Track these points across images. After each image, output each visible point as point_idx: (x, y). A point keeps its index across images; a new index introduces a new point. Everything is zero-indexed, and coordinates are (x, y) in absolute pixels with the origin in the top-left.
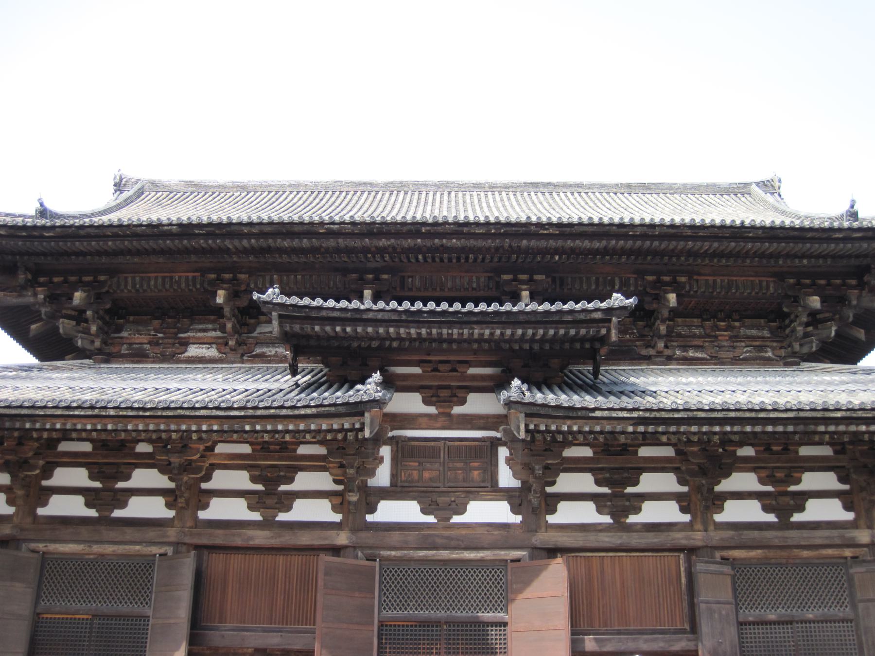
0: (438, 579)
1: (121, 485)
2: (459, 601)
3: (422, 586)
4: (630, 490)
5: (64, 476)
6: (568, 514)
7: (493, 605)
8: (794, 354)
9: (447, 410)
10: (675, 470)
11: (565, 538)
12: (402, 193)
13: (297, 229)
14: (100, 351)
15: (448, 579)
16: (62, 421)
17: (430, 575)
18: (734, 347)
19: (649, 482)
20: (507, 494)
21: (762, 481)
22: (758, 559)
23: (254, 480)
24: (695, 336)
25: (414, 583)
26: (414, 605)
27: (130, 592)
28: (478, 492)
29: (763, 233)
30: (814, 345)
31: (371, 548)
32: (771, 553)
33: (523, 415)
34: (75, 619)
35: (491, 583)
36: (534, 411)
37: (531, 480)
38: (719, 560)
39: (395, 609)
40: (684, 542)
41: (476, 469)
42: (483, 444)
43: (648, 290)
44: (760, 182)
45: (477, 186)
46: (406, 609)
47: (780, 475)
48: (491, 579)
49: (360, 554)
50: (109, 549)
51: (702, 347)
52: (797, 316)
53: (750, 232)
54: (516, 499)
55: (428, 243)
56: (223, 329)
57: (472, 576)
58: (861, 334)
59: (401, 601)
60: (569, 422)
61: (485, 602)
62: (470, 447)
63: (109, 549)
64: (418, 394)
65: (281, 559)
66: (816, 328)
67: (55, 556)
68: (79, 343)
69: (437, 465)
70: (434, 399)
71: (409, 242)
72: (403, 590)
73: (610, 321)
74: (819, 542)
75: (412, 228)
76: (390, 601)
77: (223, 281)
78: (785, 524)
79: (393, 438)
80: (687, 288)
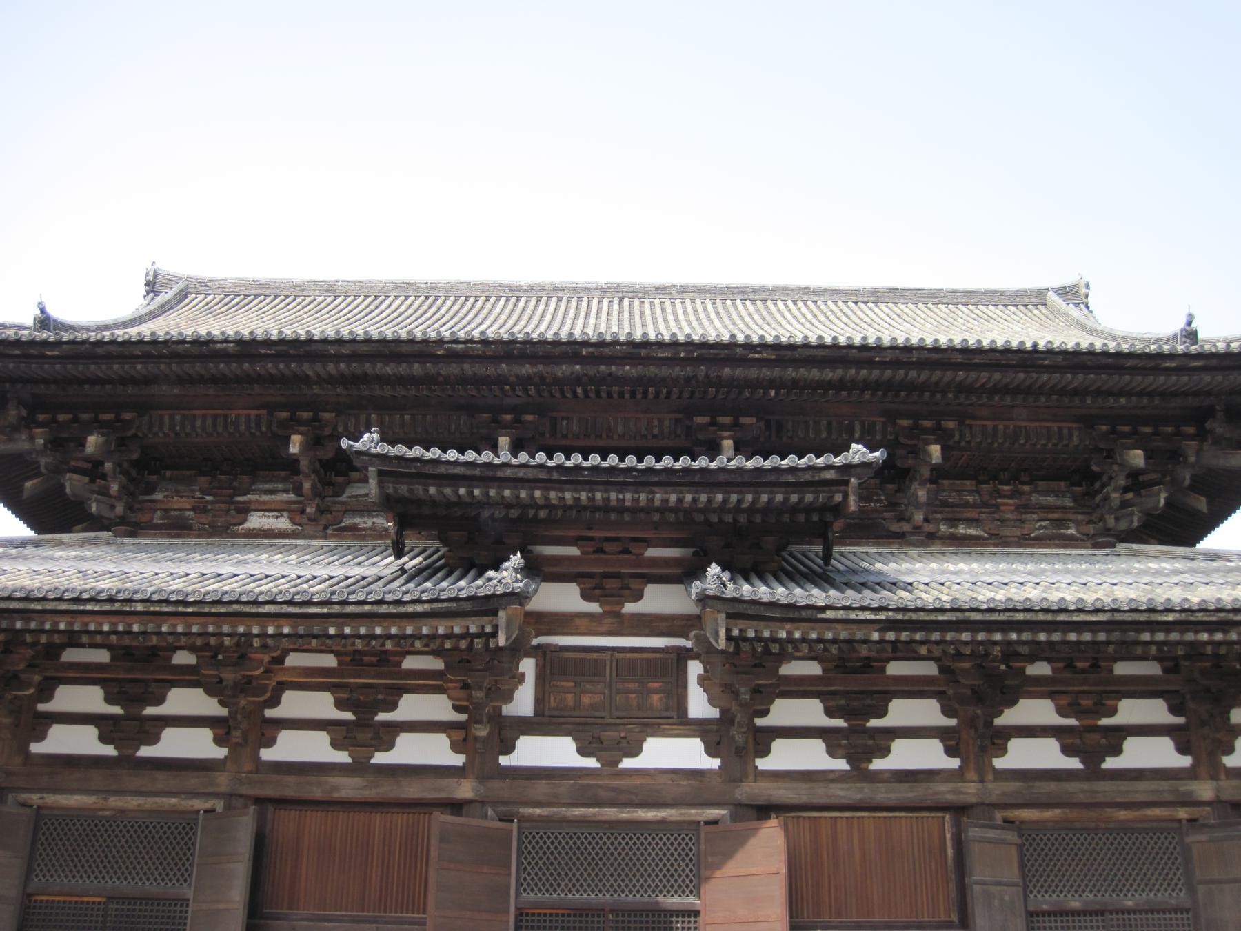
0: (601, 849)
1: (150, 711)
2: (631, 880)
3: (578, 859)
4: (874, 723)
5: (69, 698)
6: (785, 756)
7: (680, 886)
8: (1107, 531)
9: (616, 608)
10: (939, 695)
11: (781, 792)
12: (554, 299)
13: (404, 349)
14: (122, 520)
15: (616, 849)
16: (68, 618)
17: (590, 843)
18: (1022, 521)
19: (901, 712)
20: (700, 728)
21: (1061, 712)
22: (1056, 822)
23: (340, 705)
24: (967, 505)
25: (567, 853)
26: (566, 885)
27: (161, 864)
28: (659, 725)
29: (1064, 360)
30: (1135, 519)
31: (505, 803)
32: (1073, 814)
33: (724, 616)
34: (82, 902)
35: (676, 854)
36: (738, 610)
37: (735, 708)
38: (1000, 823)
39: (540, 890)
40: (951, 797)
41: (656, 691)
42: (666, 656)
43: (902, 439)
44: (1059, 289)
45: (661, 291)
46: (555, 891)
47: (1086, 702)
48: (676, 849)
49: (490, 812)
50: (133, 802)
51: (977, 520)
52: (1111, 478)
53: (1045, 359)
54: (712, 735)
55: (591, 370)
56: (298, 490)
57: (650, 844)
58: (1201, 504)
59: (548, 880)
60: (788, 626)
61: (668, 881)
62: (648, 660)
63: (133, 802)
64: (574, 585)
65: (378, 819)
66: (1138, 494)
67: (56, 812)
68: (94, 508)
69: (600, 686)
70: (597, 592)
71: (563, 370)
72: (552, 864)
73: (847, 483)
74: (1141, 798)
75: (568, 349)
76: (533, 879)
77: (299, 422)
78: (1093, 772)
79: (539, 646)
80: (957, 437)
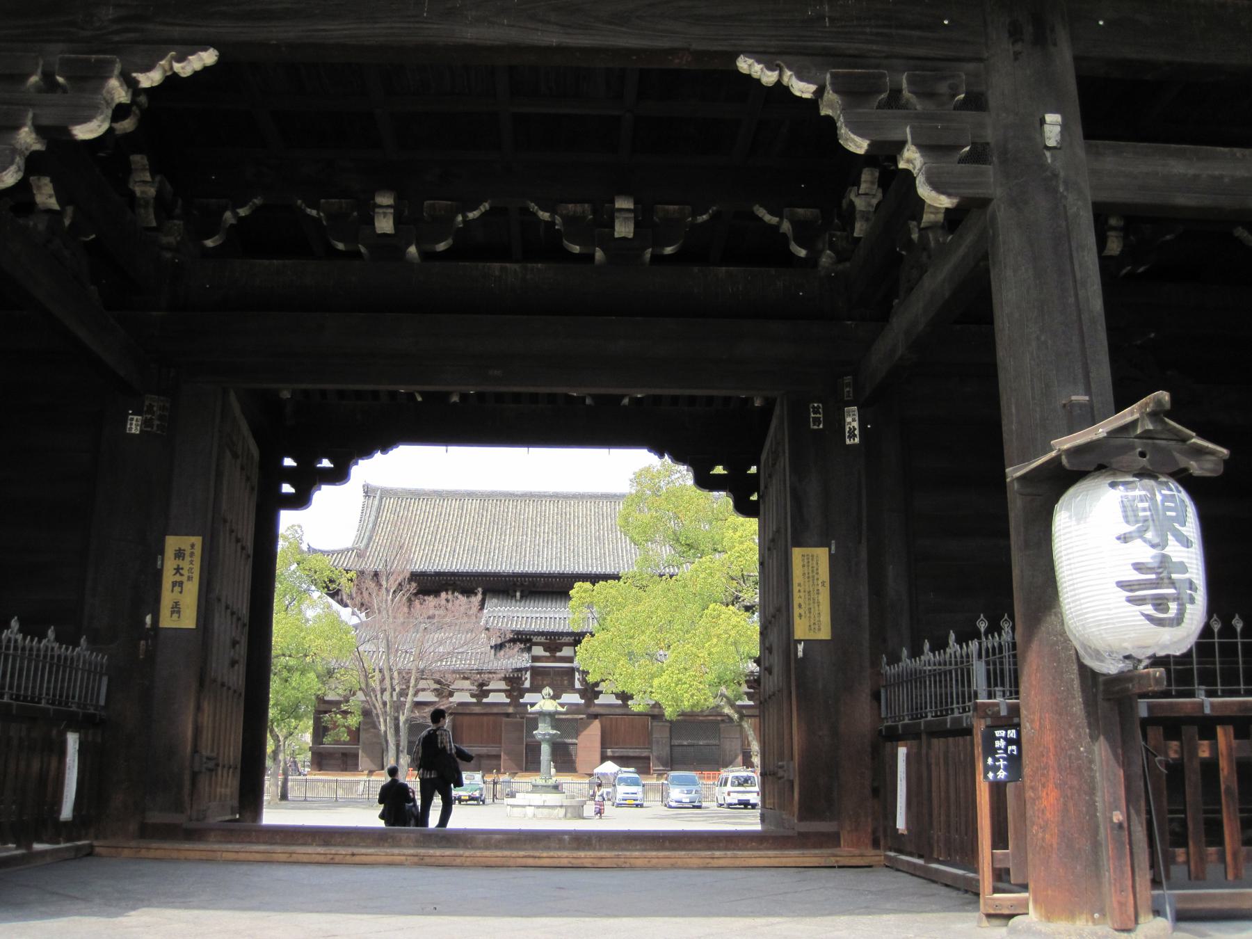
20: (578, 691)
65: (485, 718)
